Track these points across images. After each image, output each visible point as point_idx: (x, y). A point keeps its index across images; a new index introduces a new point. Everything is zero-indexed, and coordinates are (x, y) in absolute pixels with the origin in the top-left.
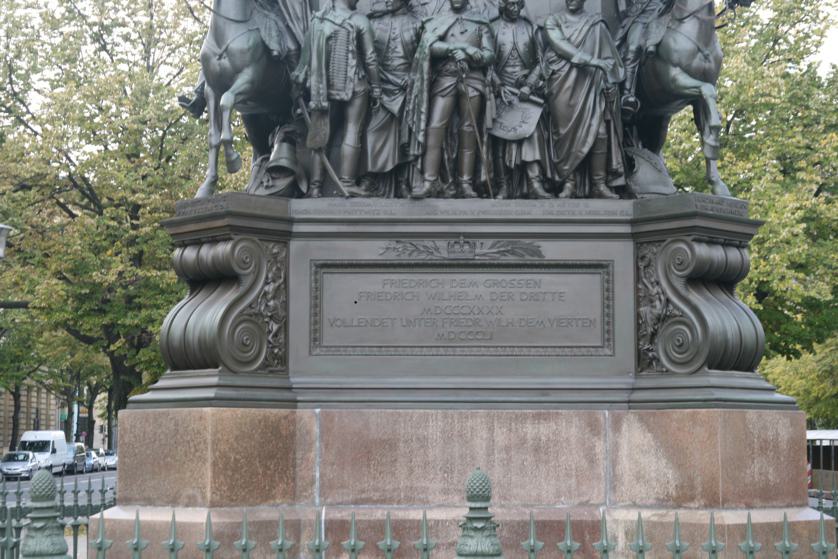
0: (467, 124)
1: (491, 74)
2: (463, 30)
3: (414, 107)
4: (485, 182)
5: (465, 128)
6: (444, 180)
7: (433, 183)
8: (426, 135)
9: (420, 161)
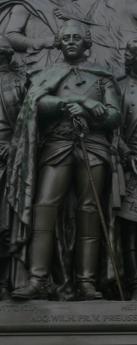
0: (87, 202)
1: (117, 141)
2: (79, 81)
3: (16, 180)
4: (113, 281)
5: (84, 208)
6: (58, 280)
7: (42, 279)
8: (32, 215)
9: (24, 251)
